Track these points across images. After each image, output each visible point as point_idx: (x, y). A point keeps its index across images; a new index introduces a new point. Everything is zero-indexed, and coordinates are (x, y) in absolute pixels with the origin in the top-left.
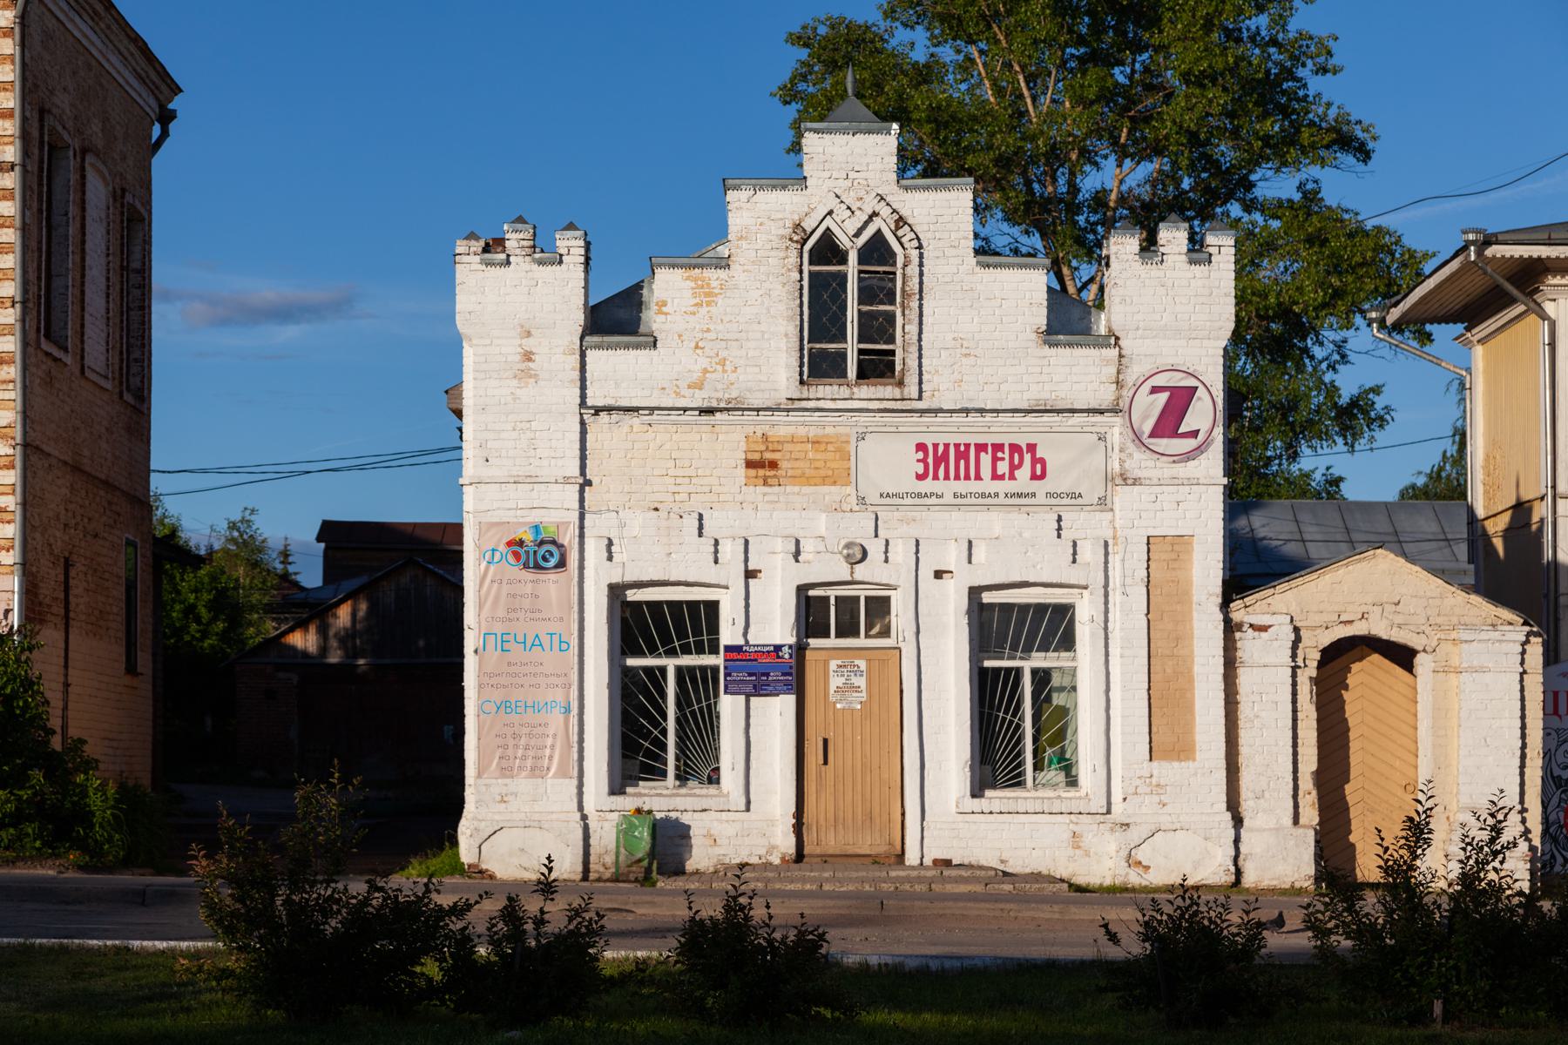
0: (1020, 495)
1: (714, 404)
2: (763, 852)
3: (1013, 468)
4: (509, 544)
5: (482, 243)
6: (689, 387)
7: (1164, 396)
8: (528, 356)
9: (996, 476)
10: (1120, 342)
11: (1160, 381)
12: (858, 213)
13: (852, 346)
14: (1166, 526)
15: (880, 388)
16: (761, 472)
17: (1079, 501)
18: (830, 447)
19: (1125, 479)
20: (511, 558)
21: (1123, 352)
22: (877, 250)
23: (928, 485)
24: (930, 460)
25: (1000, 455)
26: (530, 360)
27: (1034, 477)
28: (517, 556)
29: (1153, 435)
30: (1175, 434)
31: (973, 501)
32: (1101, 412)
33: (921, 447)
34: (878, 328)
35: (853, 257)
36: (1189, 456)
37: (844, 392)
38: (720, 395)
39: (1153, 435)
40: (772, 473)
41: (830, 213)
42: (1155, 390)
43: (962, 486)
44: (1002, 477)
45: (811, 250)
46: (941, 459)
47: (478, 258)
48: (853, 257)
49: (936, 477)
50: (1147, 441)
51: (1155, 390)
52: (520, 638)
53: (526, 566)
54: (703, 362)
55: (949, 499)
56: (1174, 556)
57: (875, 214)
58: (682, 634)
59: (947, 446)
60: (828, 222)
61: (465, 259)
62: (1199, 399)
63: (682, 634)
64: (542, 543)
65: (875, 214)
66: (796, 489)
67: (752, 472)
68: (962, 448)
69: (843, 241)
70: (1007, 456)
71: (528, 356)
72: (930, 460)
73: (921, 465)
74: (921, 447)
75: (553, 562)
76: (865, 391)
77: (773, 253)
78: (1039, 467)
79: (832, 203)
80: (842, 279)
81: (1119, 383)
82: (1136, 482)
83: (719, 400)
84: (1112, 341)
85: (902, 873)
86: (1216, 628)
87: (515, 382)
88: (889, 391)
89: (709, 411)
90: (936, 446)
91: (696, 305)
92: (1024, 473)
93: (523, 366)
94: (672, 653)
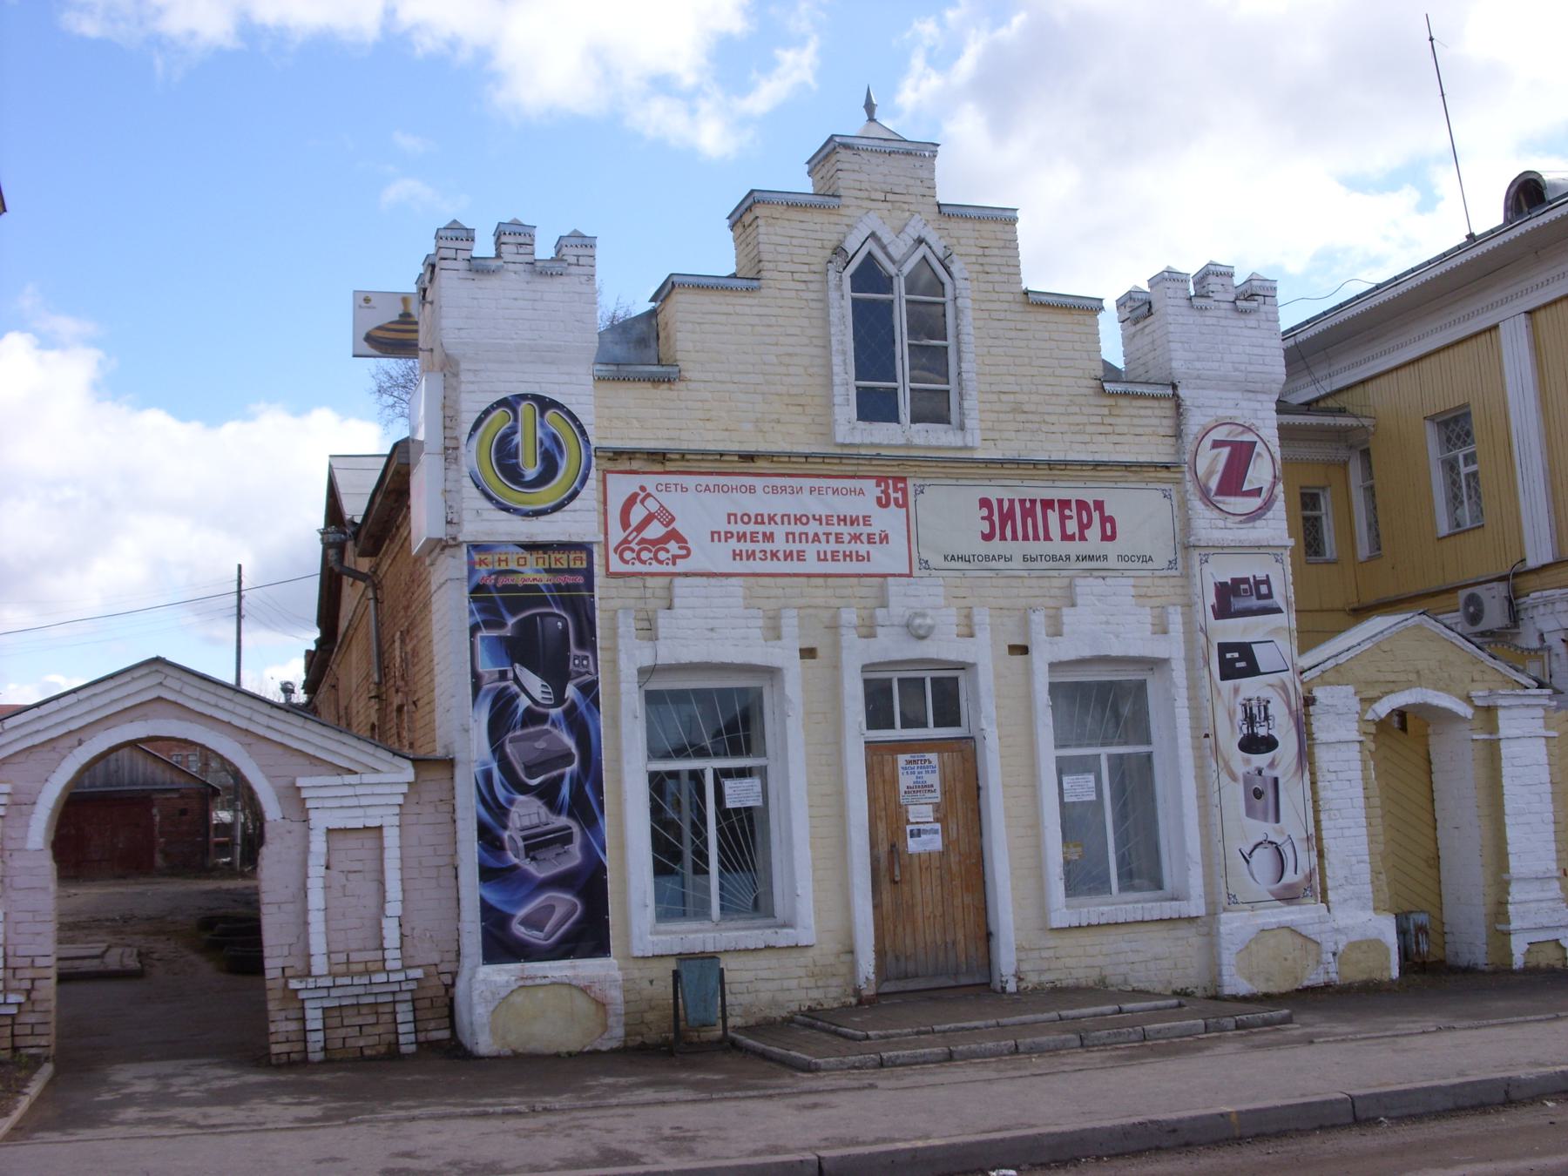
0: (1091, 558)
3: (1083, 527)
7: (1226, 451)
9: (1066, 537)
11: (1220, 434)
23: (996, 546)
24: (996, 518)
25: (1067, 512)
27: (1105, 538)
33: (985, 503)
41: (873, 235)
42: (1217, 444)
44: (1072, 538)
48: (900, 285)
49: (1003, 538)
51: (1217, 444)
59: (1011, 502)
68: (1028, 505)
72: (996, 518)
73: (987, 523)
74: (985, 503)
78: (1108, 526)
90: (1000, 502)
92: (1094, 532)
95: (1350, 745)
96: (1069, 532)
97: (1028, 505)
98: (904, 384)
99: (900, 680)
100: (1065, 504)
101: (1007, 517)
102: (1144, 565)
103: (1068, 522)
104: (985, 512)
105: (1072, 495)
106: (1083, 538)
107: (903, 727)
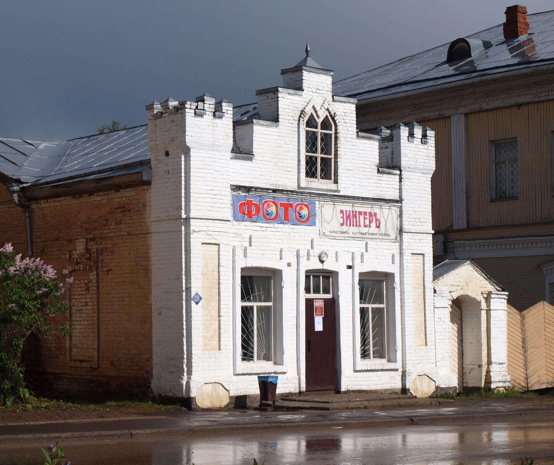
0: (372, 234)
17: (389, 238)
23: (345, 228)
33: (342, 212)
49: (347, 225)
55: (351, 235)
68: (354, 213)
73: (342, 219)
74: (342, 212)
90: (346, 211)
92: (373, 225)
94: (255, 301)
96: (366, 224)
97: (354, 213)
100: (365, 213)
101: (348, 217)
103: (366, 220)
104: (342, 215)
105: (368, 210)
106: (370, 226)
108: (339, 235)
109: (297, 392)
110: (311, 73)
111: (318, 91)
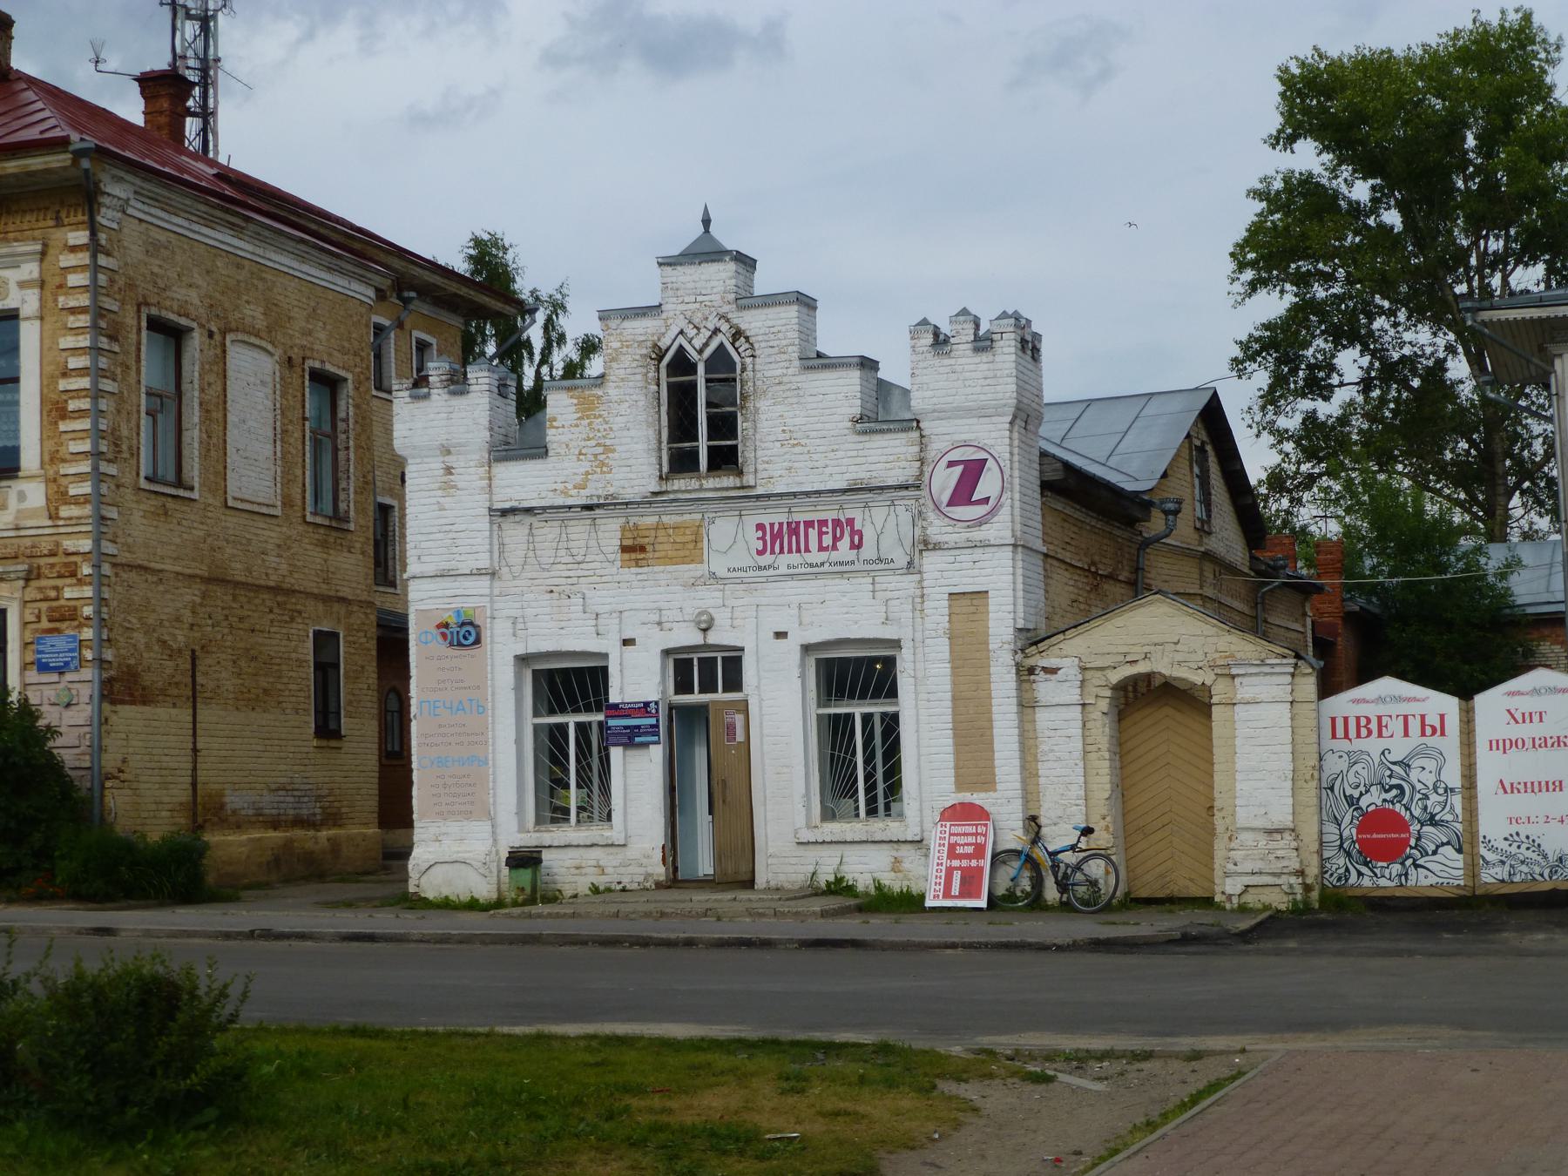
0: (841, 564)
1: (595, 501)
2: (641, 879)
3: (835, 539)
4: (439, 626)
5: (411, 380)
6: (575, 488)
7: (959, 469)
8: (449, 470)
9: (821, 548)
10: (921, 425)
11: (955, 455)
12: (703, 330)
13: (703, 445)
14: (967, 582)
15: (725, 479)
16: (633, 556)
17: (892, 566)
18: (688, 532)
19: (926, 545)
20: (440, 638)
21: (924, 433)
22: (721, 362)
23: (767, 559)
24: (768, 538)
25: (824, 529)
26: (451, 474)
27: (853, 546)
28: (444, 636)
29: (950, 504)
30: (969, 502)
31: (803, 570)
32: (906, 487)
33: (760, 527)
34: (724, 425)
35: (701, 369)
36: (980, 522)
37: (694, 484)
38: (600, 492)
39: (950, 504)
40: (642, 556)
41: (681, 332)
42: (951, 464)
43: (795, 558)
44: (826, 549)
45: (668, 365)
46: (775, 536)
47: (406, 394)
48: (701, 369)
49: (773, 552)
50: (946, 510)
51: (951, 464)
52: (448, 705)
53: (451, 644)
54: (585, 466)
55: (783, 570)
56: (972, 609)
57: (716, 331)
58: (585, 696)
59: (781, 524)
60: (681, 340)
61: (401, 394)
62: (989, 469)
63: (585, 696)
64: (463, 624)
65: (716, 331)
66: (662, 568)
67: (626, 556)
68: (794, 525)
69: (693, 355)
70: (830, 530)
71: (449, 470)
72: (768, 538)
73: (761, 542)
74: (760, 527)
75: (472, 639)
76: (710, 483)
77: (637, 370)
78: (856, 538)
79: (682, 324)
80: (694, 385)
81: (922, 461)
82: (937, 547)
83: (599, 497)
84: (915, 424)
85: (753, 897)
86: (1009, 673)
87: (440, 493)
88: (729, 481)
89: (589, 508)
90: (772, 525)
91: (579, 419)
92: (844, 543)
93: (445, 479)
94: (577, 710)
95: (190, 739)
98: (703, 445)
99: (723, 658)
100: (823, 523)
101: (775, 536)
102: (887, 566)
104: (760, 534)
105: (830, 516)
106: (834, 547)
107: (700, 692)
108: (751, 573)
109: (631, 876)
110: (679, 268)
111: (700, 298)
